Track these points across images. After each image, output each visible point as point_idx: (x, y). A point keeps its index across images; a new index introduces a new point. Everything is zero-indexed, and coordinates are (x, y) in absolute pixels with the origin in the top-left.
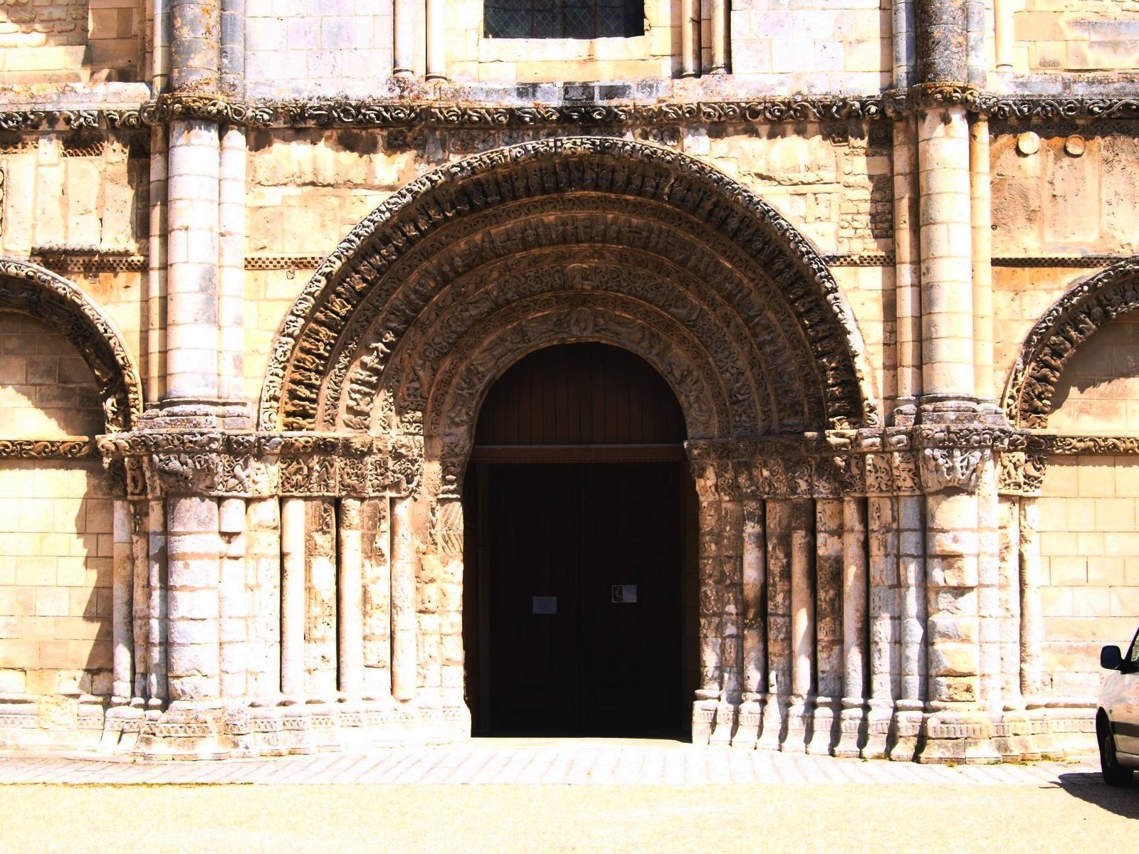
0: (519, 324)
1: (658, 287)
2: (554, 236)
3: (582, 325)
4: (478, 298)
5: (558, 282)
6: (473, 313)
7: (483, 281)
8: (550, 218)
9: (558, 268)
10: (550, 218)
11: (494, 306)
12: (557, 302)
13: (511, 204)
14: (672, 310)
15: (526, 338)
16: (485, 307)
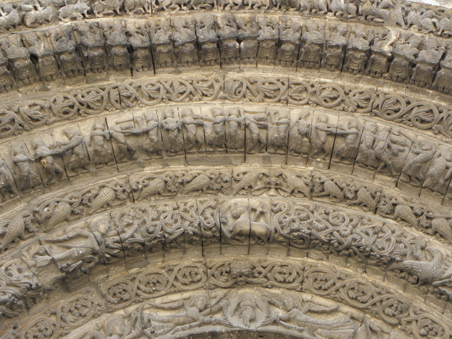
0: (137, 310)
1: (377, 232)
2: (209, 131)
3: (248, 313)
4: (71, 234)
5: (211, 219)
6: (57, 256)
7: (82, 207)
8: (203, 109)
9: (213, 203)
10: (203, 109)
11: (97, 248)
12: (206, 273)
13: (145, 79)
14: (408, 262)
15: (148, 331)
16: (80, 247)
